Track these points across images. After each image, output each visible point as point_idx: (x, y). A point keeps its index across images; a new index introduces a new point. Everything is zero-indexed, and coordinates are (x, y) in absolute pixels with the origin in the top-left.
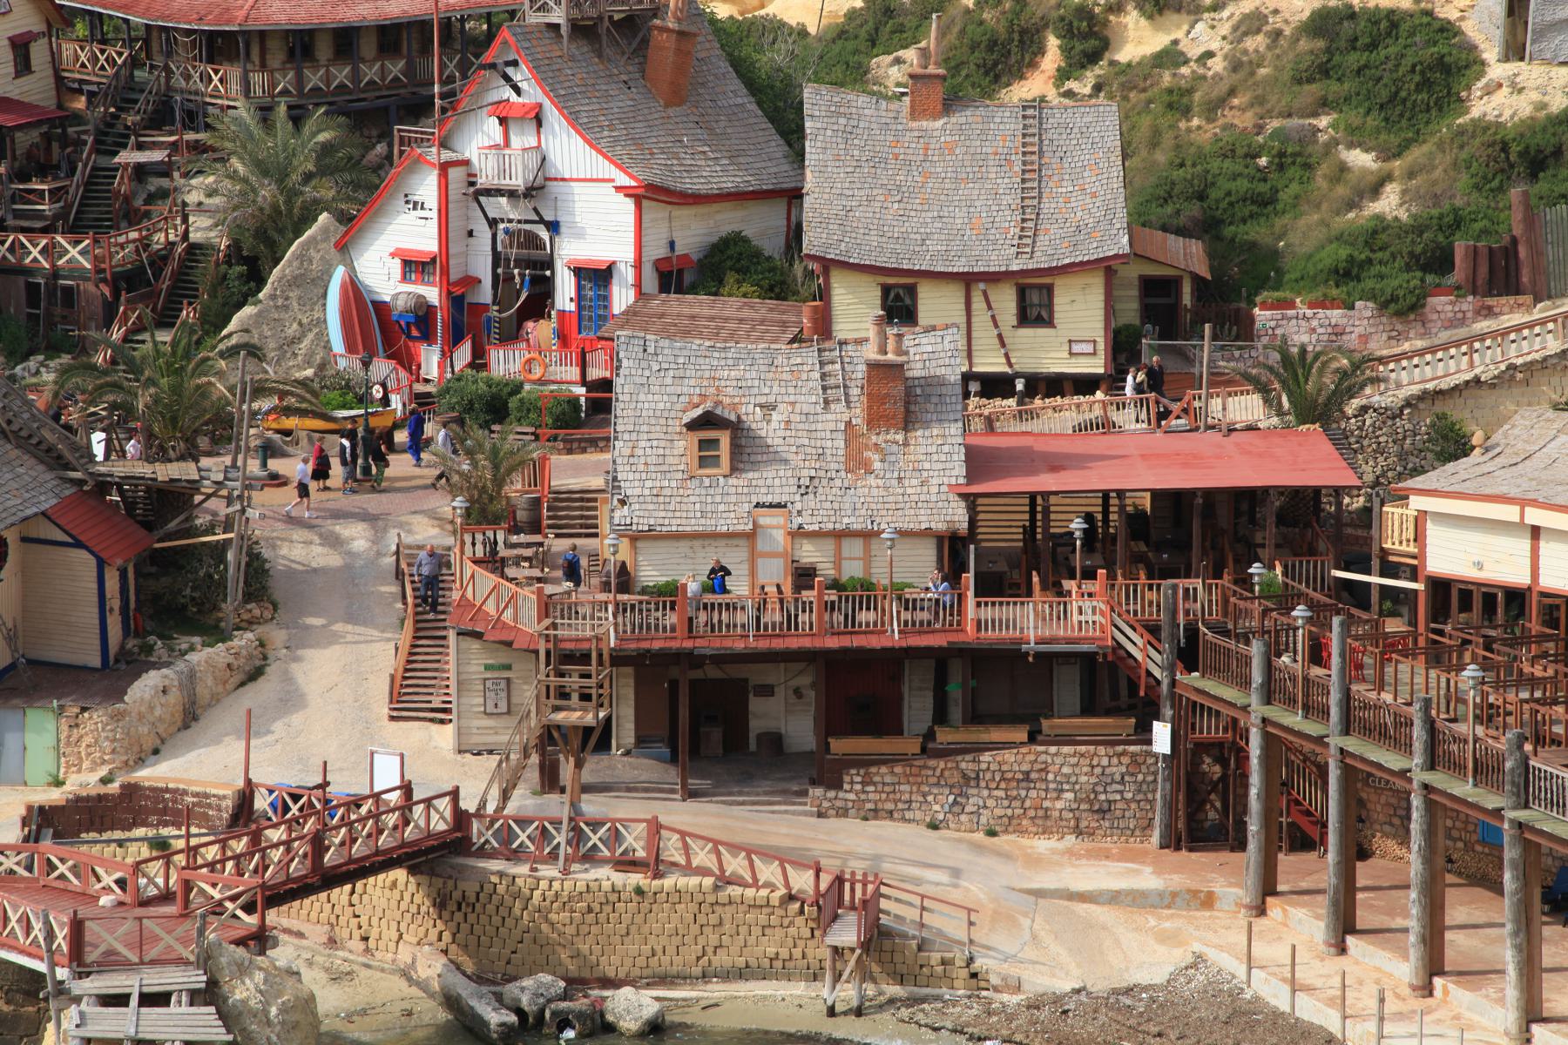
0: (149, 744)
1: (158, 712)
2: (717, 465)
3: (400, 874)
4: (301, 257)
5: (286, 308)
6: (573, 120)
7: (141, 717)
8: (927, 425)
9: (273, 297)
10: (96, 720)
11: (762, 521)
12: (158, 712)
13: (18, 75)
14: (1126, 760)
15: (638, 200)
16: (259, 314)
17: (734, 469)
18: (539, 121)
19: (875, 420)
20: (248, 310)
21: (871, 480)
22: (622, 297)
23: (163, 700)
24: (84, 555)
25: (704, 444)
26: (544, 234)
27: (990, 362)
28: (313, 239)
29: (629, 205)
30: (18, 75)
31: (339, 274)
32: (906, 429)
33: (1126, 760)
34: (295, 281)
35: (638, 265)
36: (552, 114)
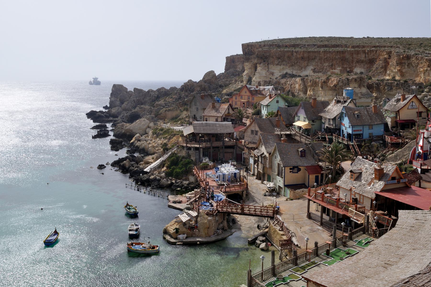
0: (298, 197)
1: (300, 194)
2: (353, 179)
4: (410, 144)
5: (406, 151)
7: (297, 193)
8: (382, 181)
9: (404, 149)
10: (292, 192)
11: (352, 189)
12: (300, 194)
16: (401, 151)
17: (355, 180)
19: (375, 178)
20: (400, 150)
21: (369, 187)
23: (302, 192)
25: (352, 175)
28: (414, 141)
32: (379, 180)
34: (409, 147)
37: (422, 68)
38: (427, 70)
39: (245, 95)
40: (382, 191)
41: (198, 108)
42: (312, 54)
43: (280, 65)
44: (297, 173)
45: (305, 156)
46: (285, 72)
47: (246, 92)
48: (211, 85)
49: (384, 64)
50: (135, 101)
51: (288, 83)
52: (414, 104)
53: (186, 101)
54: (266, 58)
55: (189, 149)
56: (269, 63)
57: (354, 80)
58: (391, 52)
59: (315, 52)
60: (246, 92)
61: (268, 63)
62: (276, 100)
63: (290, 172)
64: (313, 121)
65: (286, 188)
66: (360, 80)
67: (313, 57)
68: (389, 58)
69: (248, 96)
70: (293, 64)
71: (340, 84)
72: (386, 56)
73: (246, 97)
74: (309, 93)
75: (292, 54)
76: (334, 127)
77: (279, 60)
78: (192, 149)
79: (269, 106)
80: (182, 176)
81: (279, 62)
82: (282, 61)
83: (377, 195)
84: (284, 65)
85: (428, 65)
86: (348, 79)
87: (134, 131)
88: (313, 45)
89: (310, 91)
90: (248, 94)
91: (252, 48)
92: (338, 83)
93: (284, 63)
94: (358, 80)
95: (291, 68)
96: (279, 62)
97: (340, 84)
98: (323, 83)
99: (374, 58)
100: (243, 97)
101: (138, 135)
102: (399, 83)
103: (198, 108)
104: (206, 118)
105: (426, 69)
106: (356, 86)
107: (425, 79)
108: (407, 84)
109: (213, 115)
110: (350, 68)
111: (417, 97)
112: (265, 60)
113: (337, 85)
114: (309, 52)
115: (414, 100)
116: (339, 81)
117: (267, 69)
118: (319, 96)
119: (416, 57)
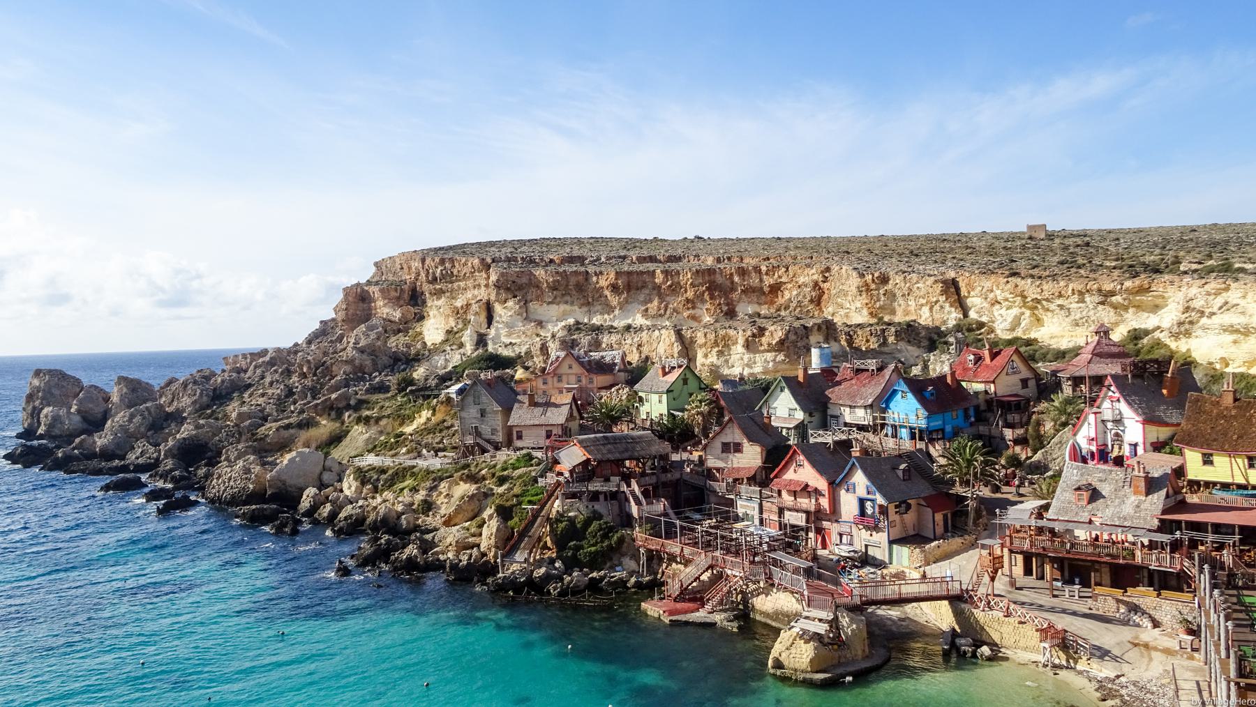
3: (946, 603)
6: (1127, 401)
13: (1023, 388)
14: (1188, 608)
15: (1144, 424)
18: (1118, 400)
22: (1140, 450)
24: (929, 509)
26: (1122, 433)
27: (1240, 480)
29: (1141, 426)
30: (1023, 388)
31: (1071, 442)
33: (1188, 608)
35: (1144, 443)
36: (1122, 400)
37: (923, 298)
38: (937, 302)
39: (568, 374)
40: (1164, 512)
41: (485, 410)
42: (635, 276)
43: (558, 304)
44: (906, 513)
45: (910, 479)
46: (571, 321)
47: (570, 367)
48: (377, 357)
49: (814, 294)
50: (152, 410)
51: (629, 341)
52: (1015, 365)
53: (336, 399)
54: (520, 288)
55: (595, 496)
56: (528, 300)
57: (816, 327)
58: (828, 269)
59: (642, 273)
60: (570, 367)
61: (526, 301)
62: (682, 376)
63: (896, 512)
64: (811, 415)
65: (895, 546)
66: (827, 328)
67: (640, 285)
68: (824, 282)
69: (576, 374)
70: (590, 300)
71: (792, 337)
72: (815, 277)
73: (573, 379)
74: (704, 360)
75: (587, 280)
76: (871, 423)
77: (555, 292)
78: (602, 497)
79: (672, 391)
80: (605, 564)
81: (555, 298)
82: (563, 295)
83: (1161, 521)
84: (566, 303)
85: (941, 291)
86: (805, 328)
87: (290, 482)
88: (620, 257)
89: (706, 356)
90: (577, 369)
91: (453, 266)
92: (787, 335)
93: (568, 298)
94: (824, 327)
95: (585, 309)
96: (555, 298)
97: (792, 337)
98: (750, 339)
99: (781, 282)
100: (564, 378)
101: (311, 491)
102: (899, 329)
103: (485, 410)
104: (517, 432)
105: (935, 299)
106: (822, 340)
107: (933, 320)
108: (912, 331)
109: (537, 423)
110: (728, 304)
111: (1019, 352)
112: (516, 293)
113: (784, 340)
114: (629, 273)
115: (1015, 358)
116: (789, 332)
117: (525, 314)
118: (733, 366)
119: (905, 277)
